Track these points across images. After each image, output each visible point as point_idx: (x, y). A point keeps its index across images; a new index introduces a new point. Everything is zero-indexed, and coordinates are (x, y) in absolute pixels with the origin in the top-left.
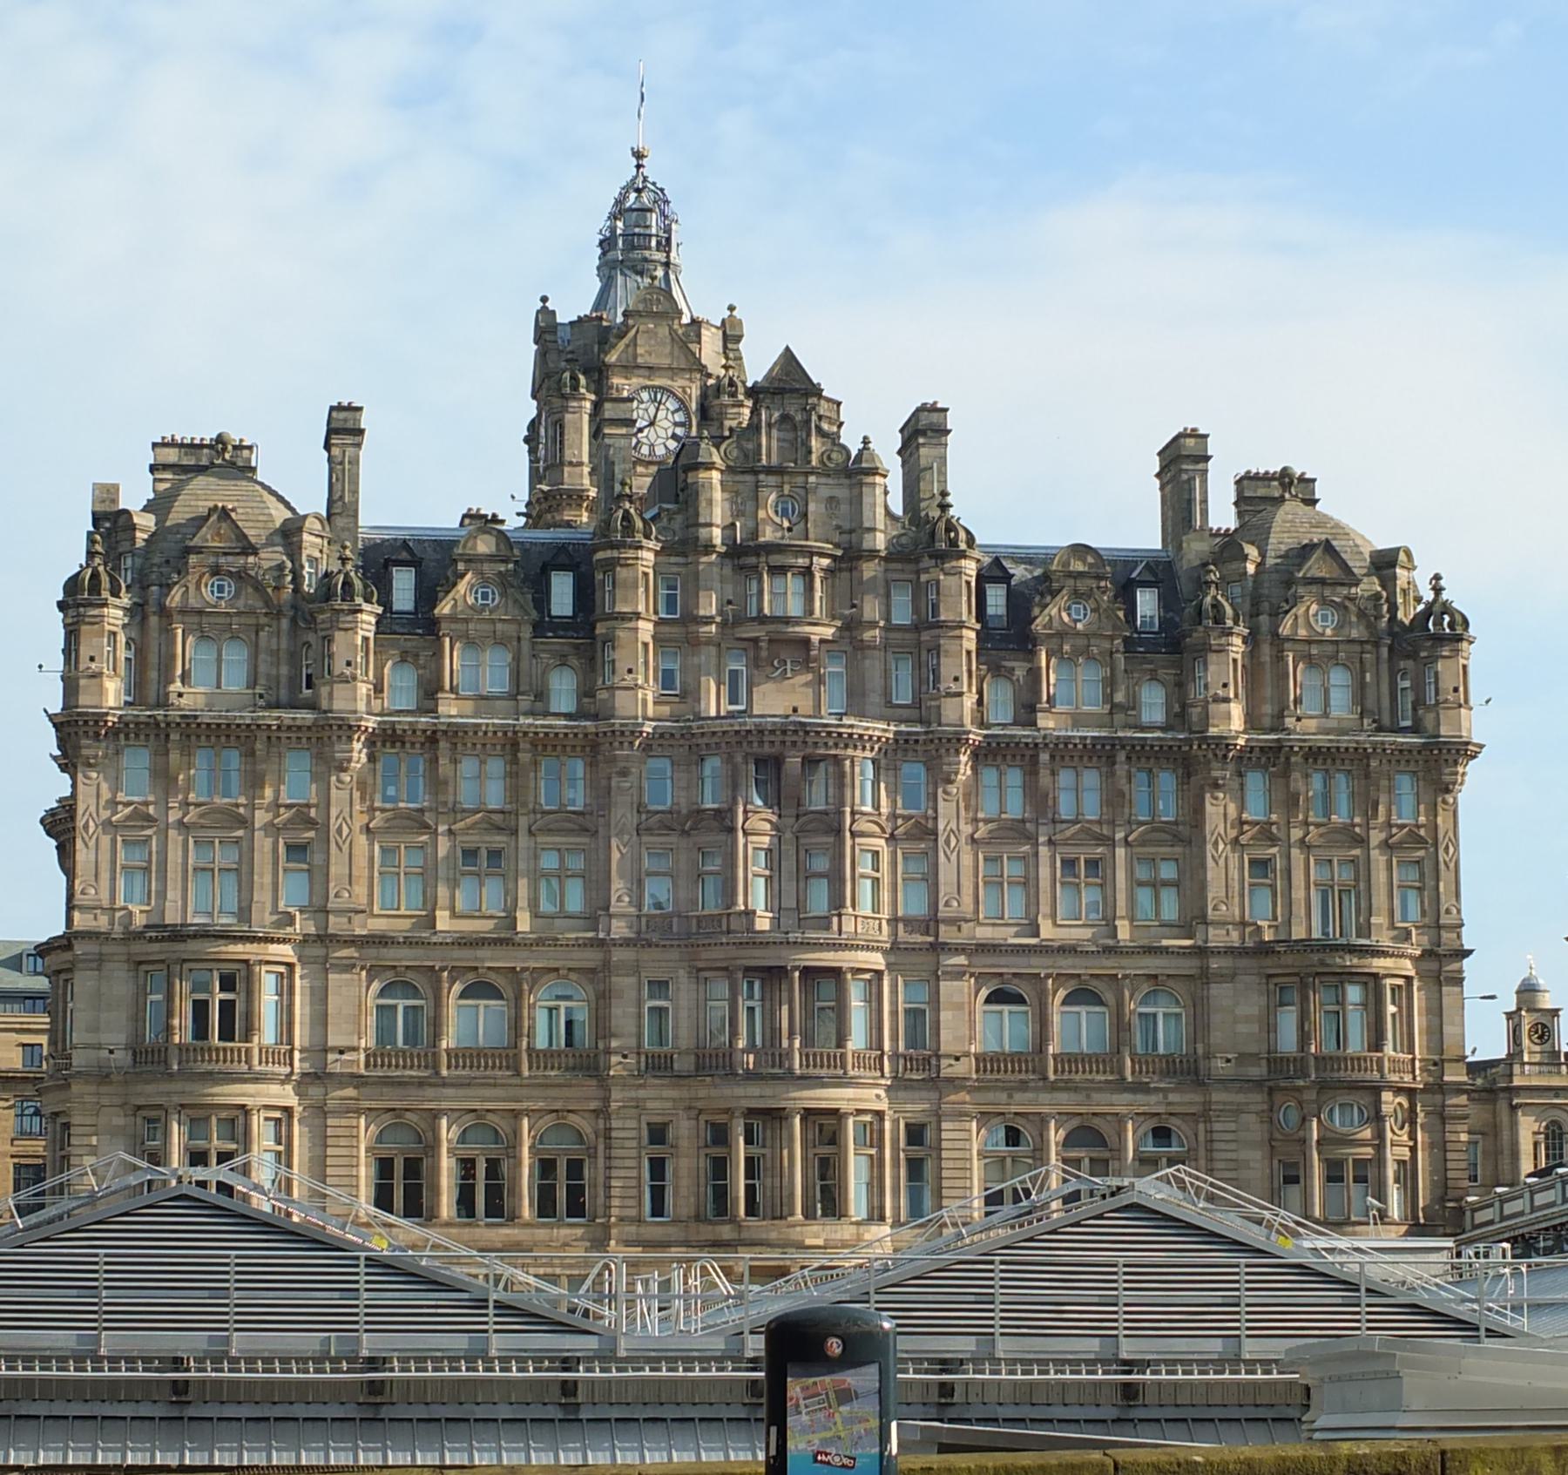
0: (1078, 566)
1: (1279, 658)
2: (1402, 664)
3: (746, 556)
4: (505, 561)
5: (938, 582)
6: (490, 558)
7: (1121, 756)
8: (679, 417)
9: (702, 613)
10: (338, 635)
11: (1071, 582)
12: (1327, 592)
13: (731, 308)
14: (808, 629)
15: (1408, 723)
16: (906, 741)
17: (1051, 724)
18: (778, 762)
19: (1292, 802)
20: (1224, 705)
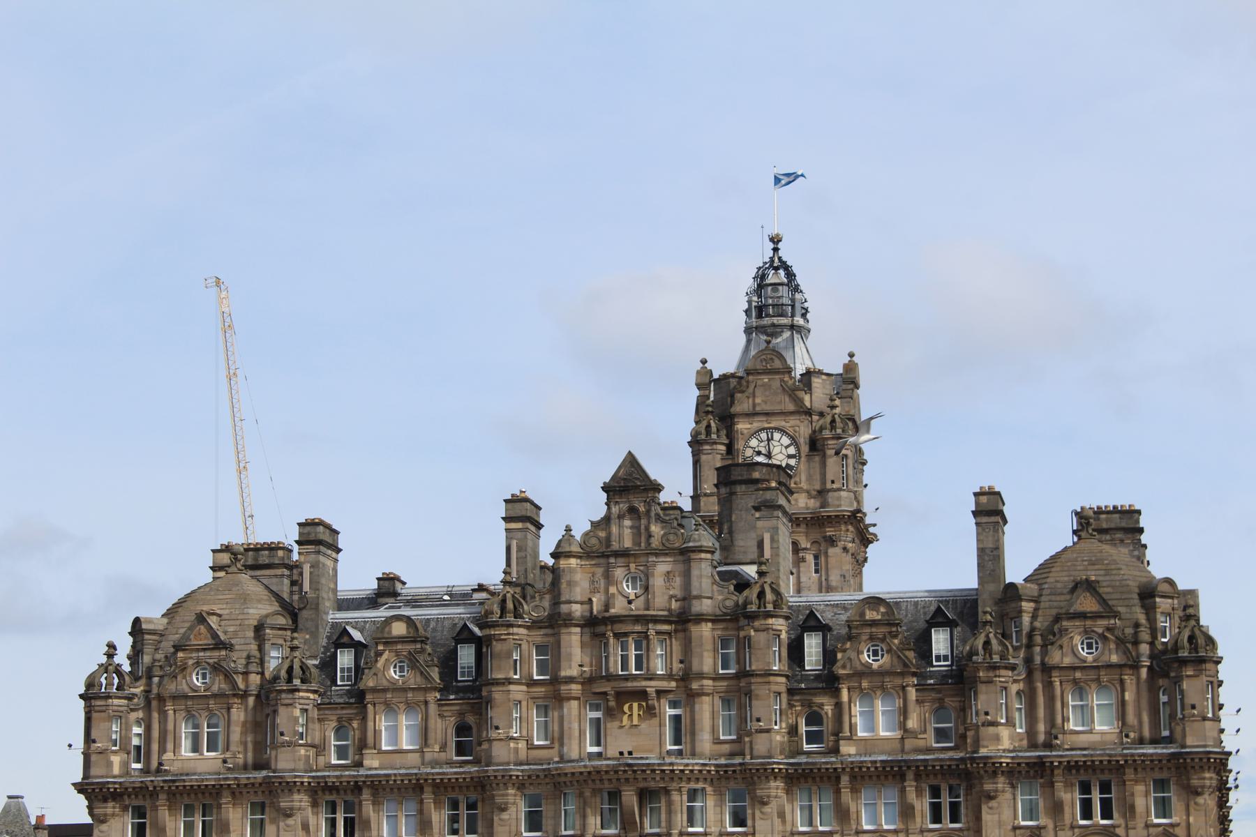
0: (870, 615)
1: (1049, 685)
2: (1161, 682)
3: (598, 626)
4: (415, 642)
5: (750, 638)
6: (401, 640)
7: (910, 775)
8: (792, 450)
9: (563, 674)
10: (282, 710)
11: (868, 630)
12: (1089, 623)
13: (851, 355)
14: (644, 683)
15: (1166, 733)
16: (726, 772)
17: (852, 750)
18: (614, 796)
19: (1056, 809)
20: (991, 729)
